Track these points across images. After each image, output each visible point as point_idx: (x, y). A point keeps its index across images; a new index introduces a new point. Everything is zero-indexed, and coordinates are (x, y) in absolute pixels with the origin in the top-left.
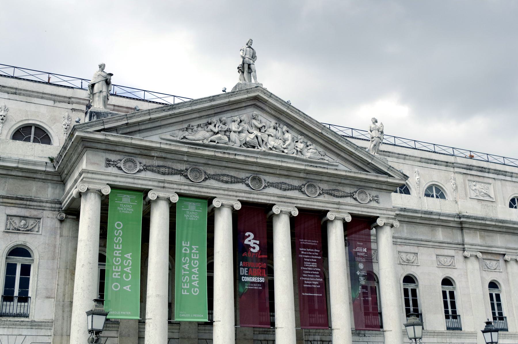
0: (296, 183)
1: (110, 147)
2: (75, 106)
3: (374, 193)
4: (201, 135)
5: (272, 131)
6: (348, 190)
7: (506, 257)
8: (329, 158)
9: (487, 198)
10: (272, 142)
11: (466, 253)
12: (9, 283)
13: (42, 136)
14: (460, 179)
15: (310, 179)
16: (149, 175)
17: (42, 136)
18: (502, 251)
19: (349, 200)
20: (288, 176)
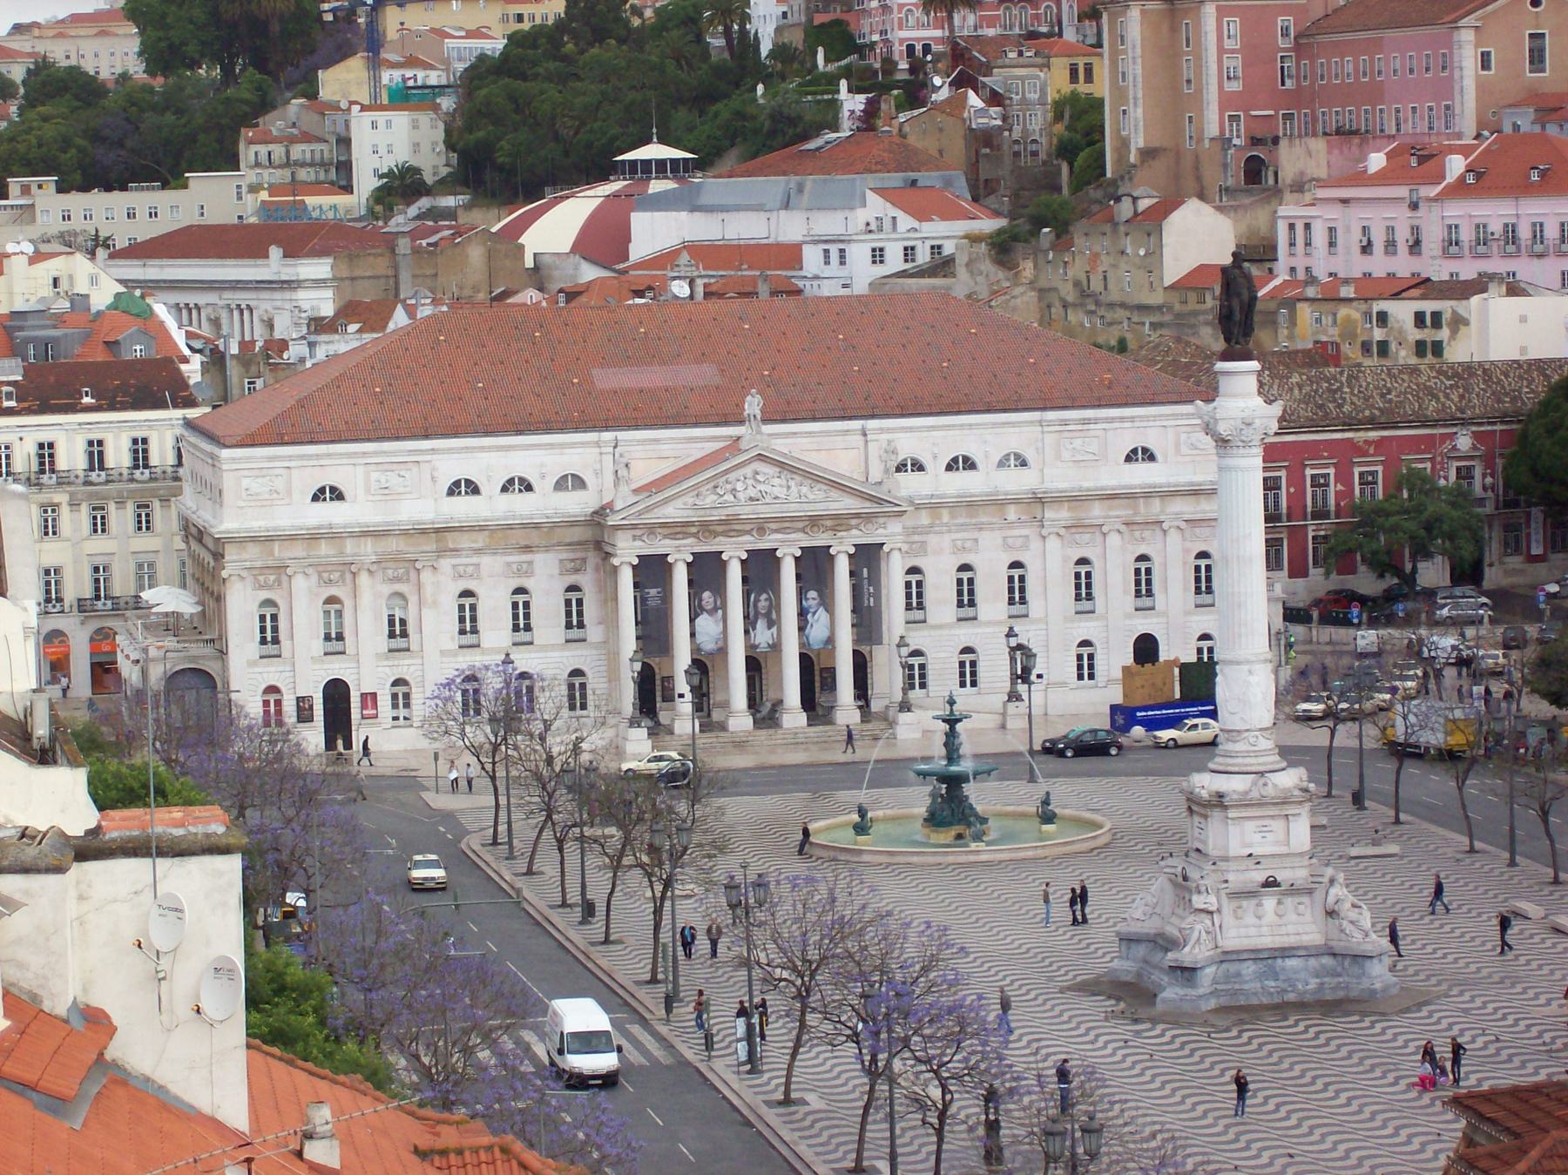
0: (800, 525)
1: (634, 527)
2: (604, 450)
3: (881, 520)
4: (710, 499)
5: (776, 481)
6: (853, 522)
7: (1105, 529)
8: (835, 494)
9: (1091, 457)
10: (777, 491)
11: (1044, 532)
12: (569, 614)
13: (579, 483)
14: (1050, 439)
15: (814, 522)
16: (667, 541)
17: (579, 483)
18: (1100, 521)
19: (854, 532)
20: (786, 523)
